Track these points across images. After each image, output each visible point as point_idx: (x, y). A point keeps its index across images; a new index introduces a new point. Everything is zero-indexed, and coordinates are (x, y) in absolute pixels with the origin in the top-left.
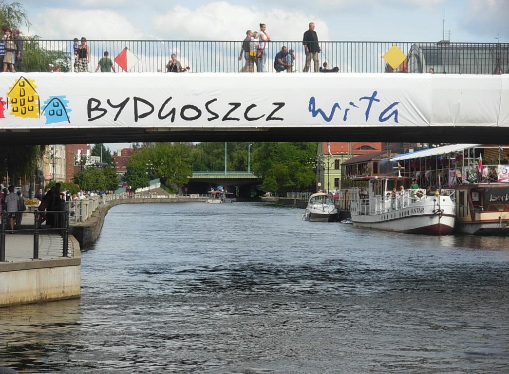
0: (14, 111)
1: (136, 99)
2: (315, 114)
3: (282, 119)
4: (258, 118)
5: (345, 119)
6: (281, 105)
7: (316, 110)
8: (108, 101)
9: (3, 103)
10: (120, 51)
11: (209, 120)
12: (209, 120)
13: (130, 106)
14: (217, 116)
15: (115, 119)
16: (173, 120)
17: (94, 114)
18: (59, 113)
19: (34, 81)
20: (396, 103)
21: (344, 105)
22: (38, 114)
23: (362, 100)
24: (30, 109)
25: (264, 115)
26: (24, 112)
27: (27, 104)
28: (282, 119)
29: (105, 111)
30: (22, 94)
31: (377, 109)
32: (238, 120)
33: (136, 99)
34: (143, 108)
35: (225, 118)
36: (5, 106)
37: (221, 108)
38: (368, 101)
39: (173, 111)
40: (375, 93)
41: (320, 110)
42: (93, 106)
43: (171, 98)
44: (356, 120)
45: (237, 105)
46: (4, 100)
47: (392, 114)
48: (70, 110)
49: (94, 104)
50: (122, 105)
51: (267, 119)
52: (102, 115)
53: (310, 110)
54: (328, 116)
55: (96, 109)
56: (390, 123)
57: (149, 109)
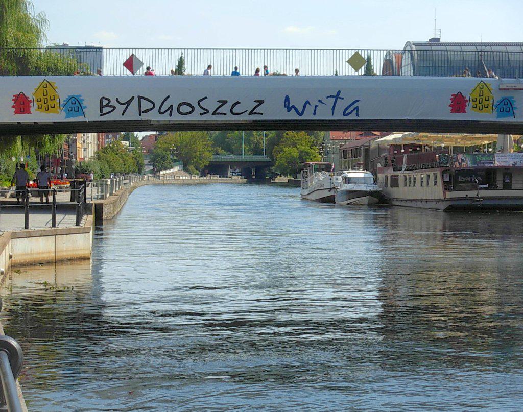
0: (39, 108)
2: (289, 110)
3: (262, 114)
4: (243, 113)
5: (314, 114)
6: (261, 102)
7: (290, 106)
8: (117, 100)
9: (30, 101)
10: (128, 57)
11: (201, 114)
12: (201, 114)
13: (135, 103)
14: (208, 112)
15: (123, 114)
16: (170, 115)
17: (105, 110)
18: (76, 109)
19: (55, 83)
20: (357, 101)
21: (314, 103)
22: (59, 110)
23: (329, 98)
24: (52, 106)
25: (247, 111)
26: (47, 109)
27: (50, 102)
28: (262, 114)
29: (115, 108)
30: (45, 94)
31: (341, 105)
32: (225, 114)
34: (146, 105)
36: (31, 104)
37: (211, 105)
38: (334, 98)
39: (171, 107)
40: (339, 92)
41: (293, 107)
43: (169, 96)
44: (324, 114)
45: (224, 102)
46: (31, 99)
47: (354, 109)
48: (85, 107)
49: (105, 102)
50: (129, 103)
51: (249, 114)
52: (112, 111)
53: (285, 107)
54: (300, 111)
55: (107, 106)
56: (352, 117)
57: (151, 106)
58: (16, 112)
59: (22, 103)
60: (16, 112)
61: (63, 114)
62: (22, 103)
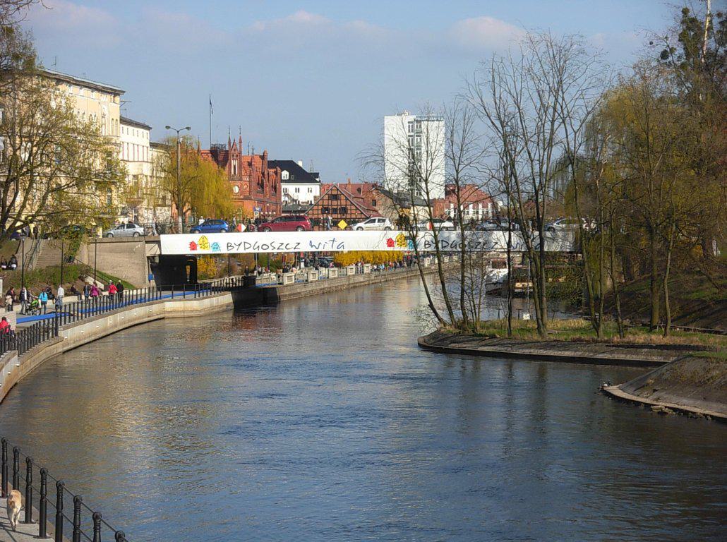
2: (312, 246)
6: (299, 244)
13: (242, 245)
17: (230, 248)
21: (323, 243)
31: (336, 245)
37: (276, 245)
45: (282, 244)
49: (229, 245)
50: (239, 245)
59: (193, 246)
62: (193, 246)
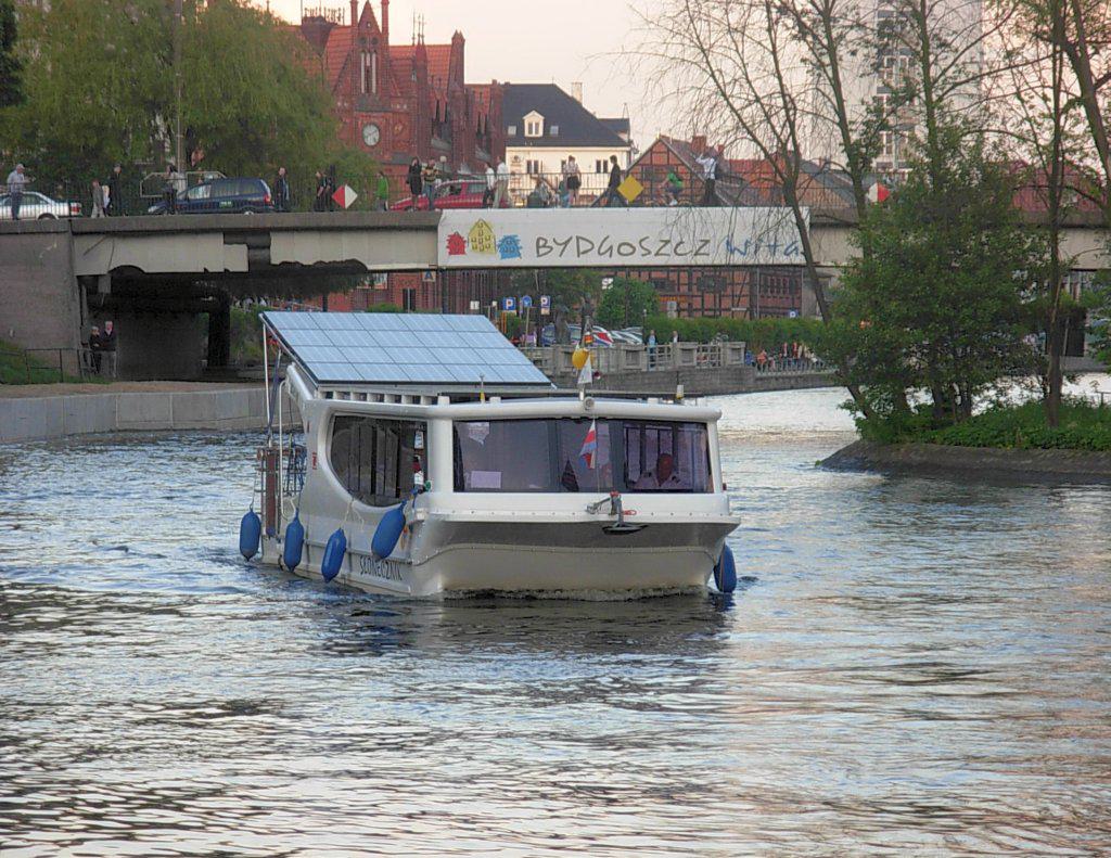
1: (578, 238)
2: (732, 252)
6: (707, 242)
13: (573, 244)
14: (649, 253)
16: (611, 256)
17: (542, 251)
29: (552, 249)
33: (578, 238)
34: (584, 246)
35: (657, 254)
36: (466, 245)
39: (611, 248)
41: (735, 249)
42: (541, 245)
45: (667, 242)
46: (466, 239)
49: (542, 243)
50: (566, 243)
55: (544, 246)
57: (590, 246)
58: (450, 253)
60: (450, 253)
61: (499, 254)
